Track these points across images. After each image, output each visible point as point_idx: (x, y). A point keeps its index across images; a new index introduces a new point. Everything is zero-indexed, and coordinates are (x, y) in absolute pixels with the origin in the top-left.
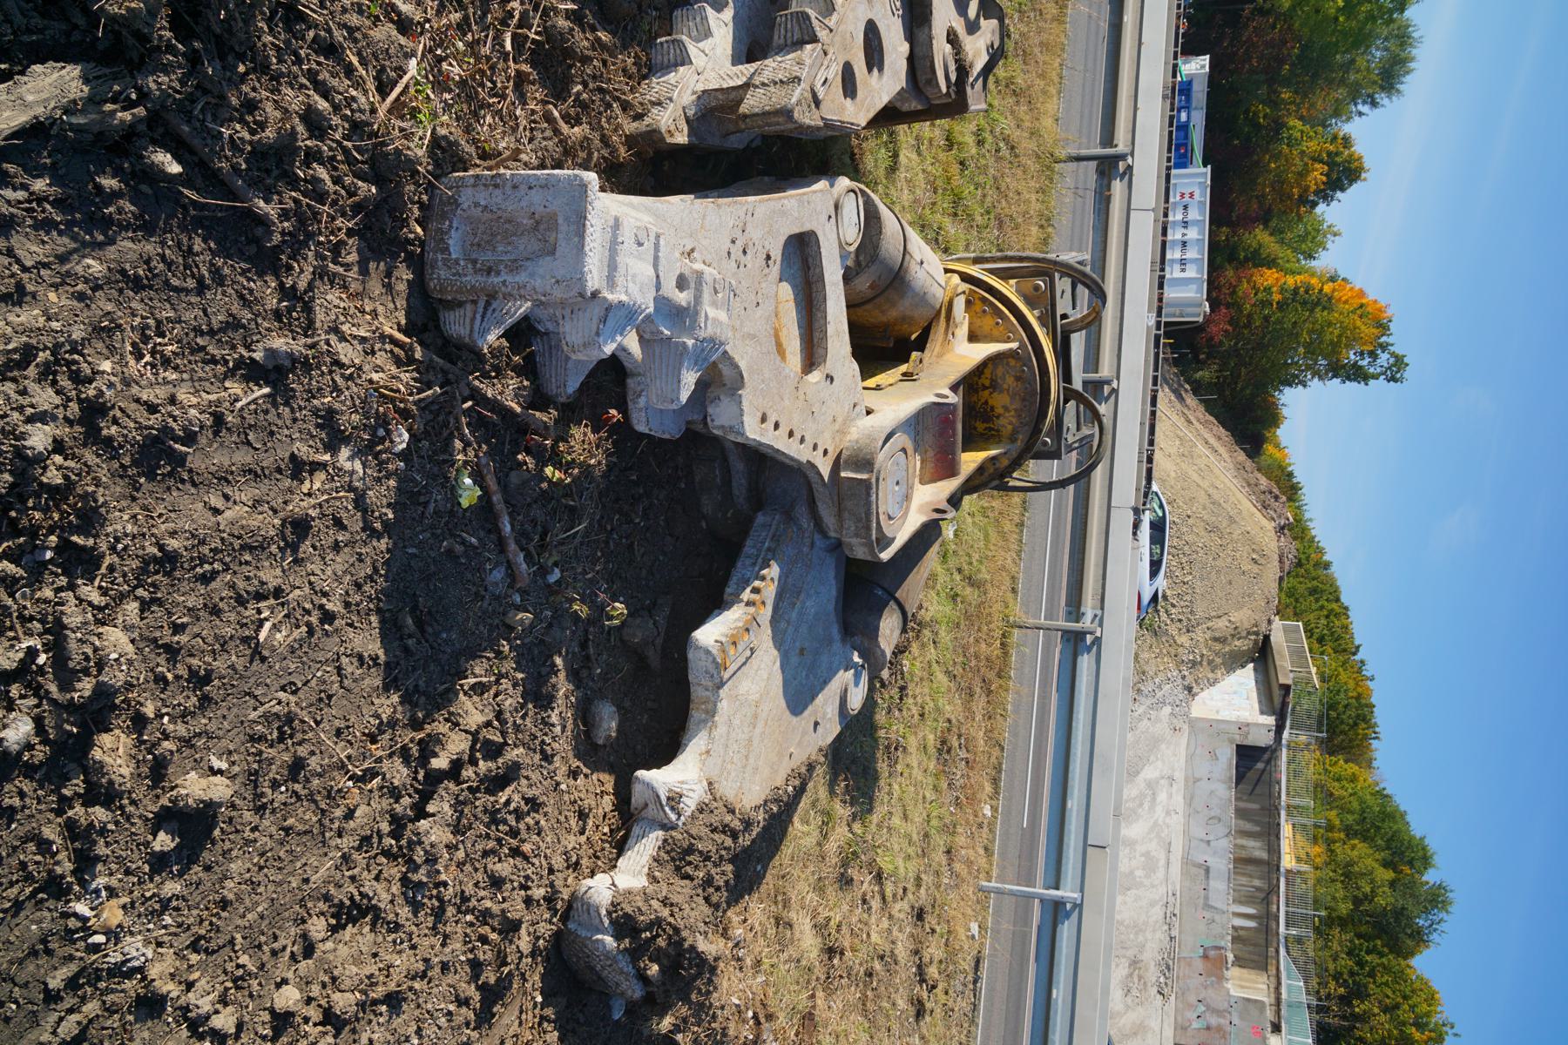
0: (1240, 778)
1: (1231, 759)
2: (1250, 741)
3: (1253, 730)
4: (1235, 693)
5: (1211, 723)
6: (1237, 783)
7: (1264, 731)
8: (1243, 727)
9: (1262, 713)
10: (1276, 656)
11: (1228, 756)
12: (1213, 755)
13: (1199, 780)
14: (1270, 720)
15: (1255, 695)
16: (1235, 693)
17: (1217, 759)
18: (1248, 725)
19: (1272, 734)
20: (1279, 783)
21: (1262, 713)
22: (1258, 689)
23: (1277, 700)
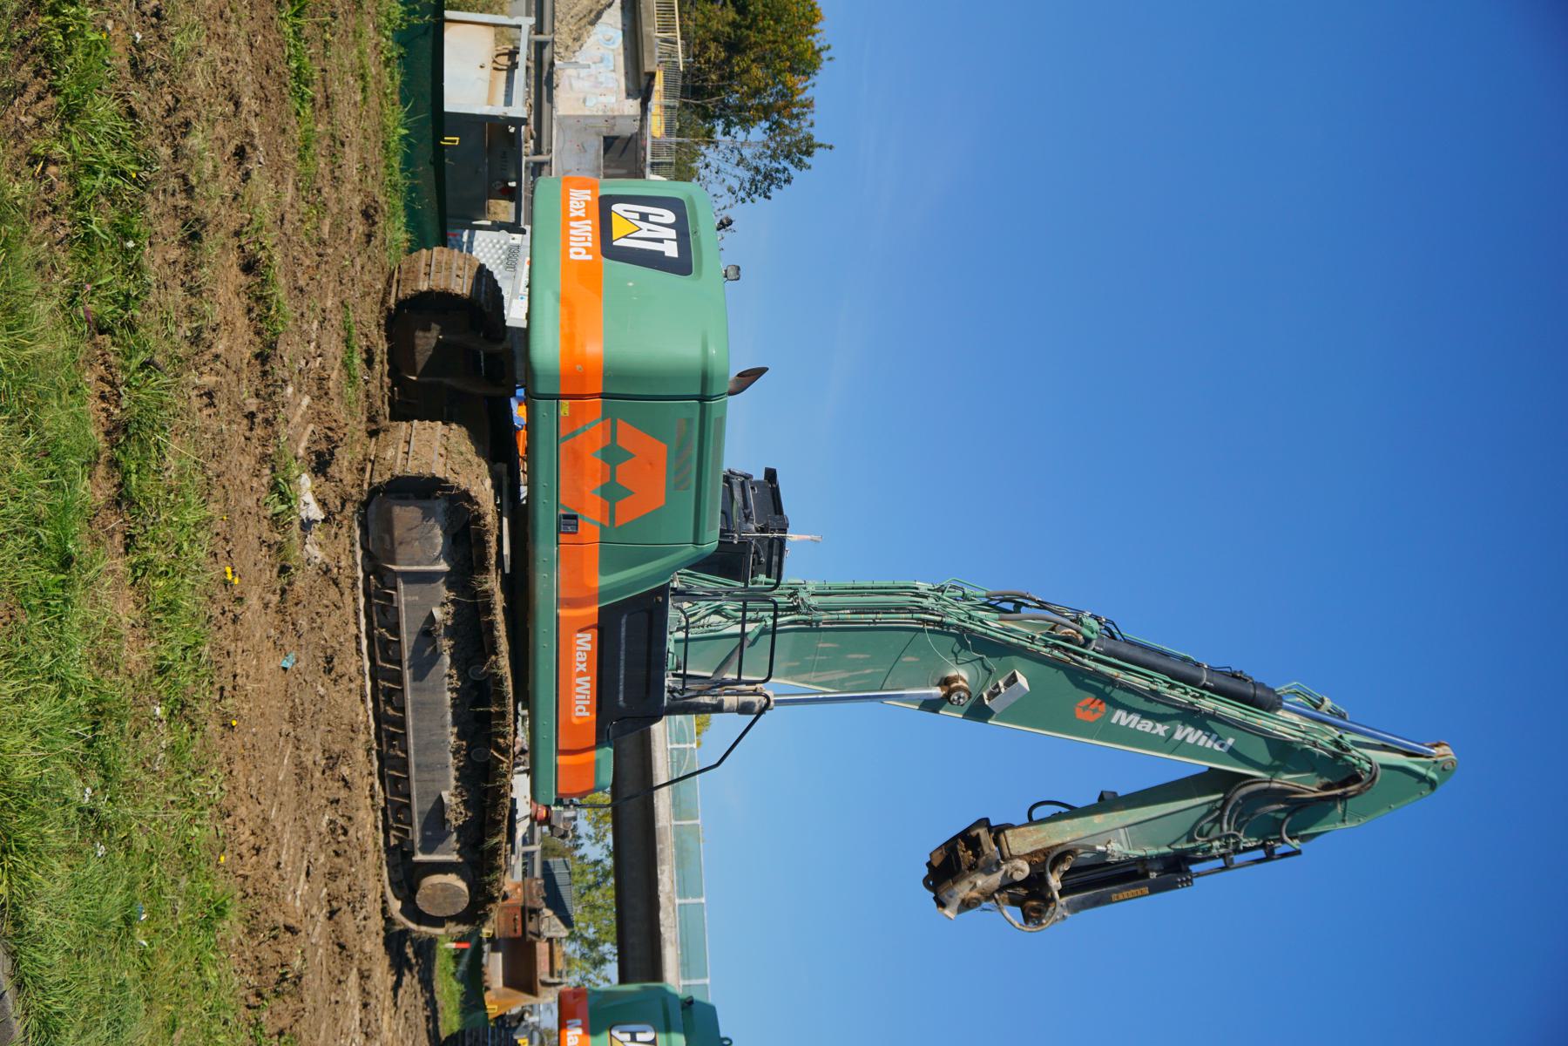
0: (606, 150)
1: (599, 150)
2: (613, 134)
3: (619, 122)
4: (602, 61)
5: (578, 118)
6: (605, 153)
7: (630, 121)
8: (610, 119)
9: (629, 95)
10: (644, 15)
11: (597, 145)
12: (583, 149)
13: (568, 172)
14: (632, 107)
15: (621, 60)
16: (602, 61)
17: (585, 151)
18: (614, 117)
19: (638, 123)
20: (644, 149)
21: (629, 95)
22: (625, 49)
23: (644, 83)
